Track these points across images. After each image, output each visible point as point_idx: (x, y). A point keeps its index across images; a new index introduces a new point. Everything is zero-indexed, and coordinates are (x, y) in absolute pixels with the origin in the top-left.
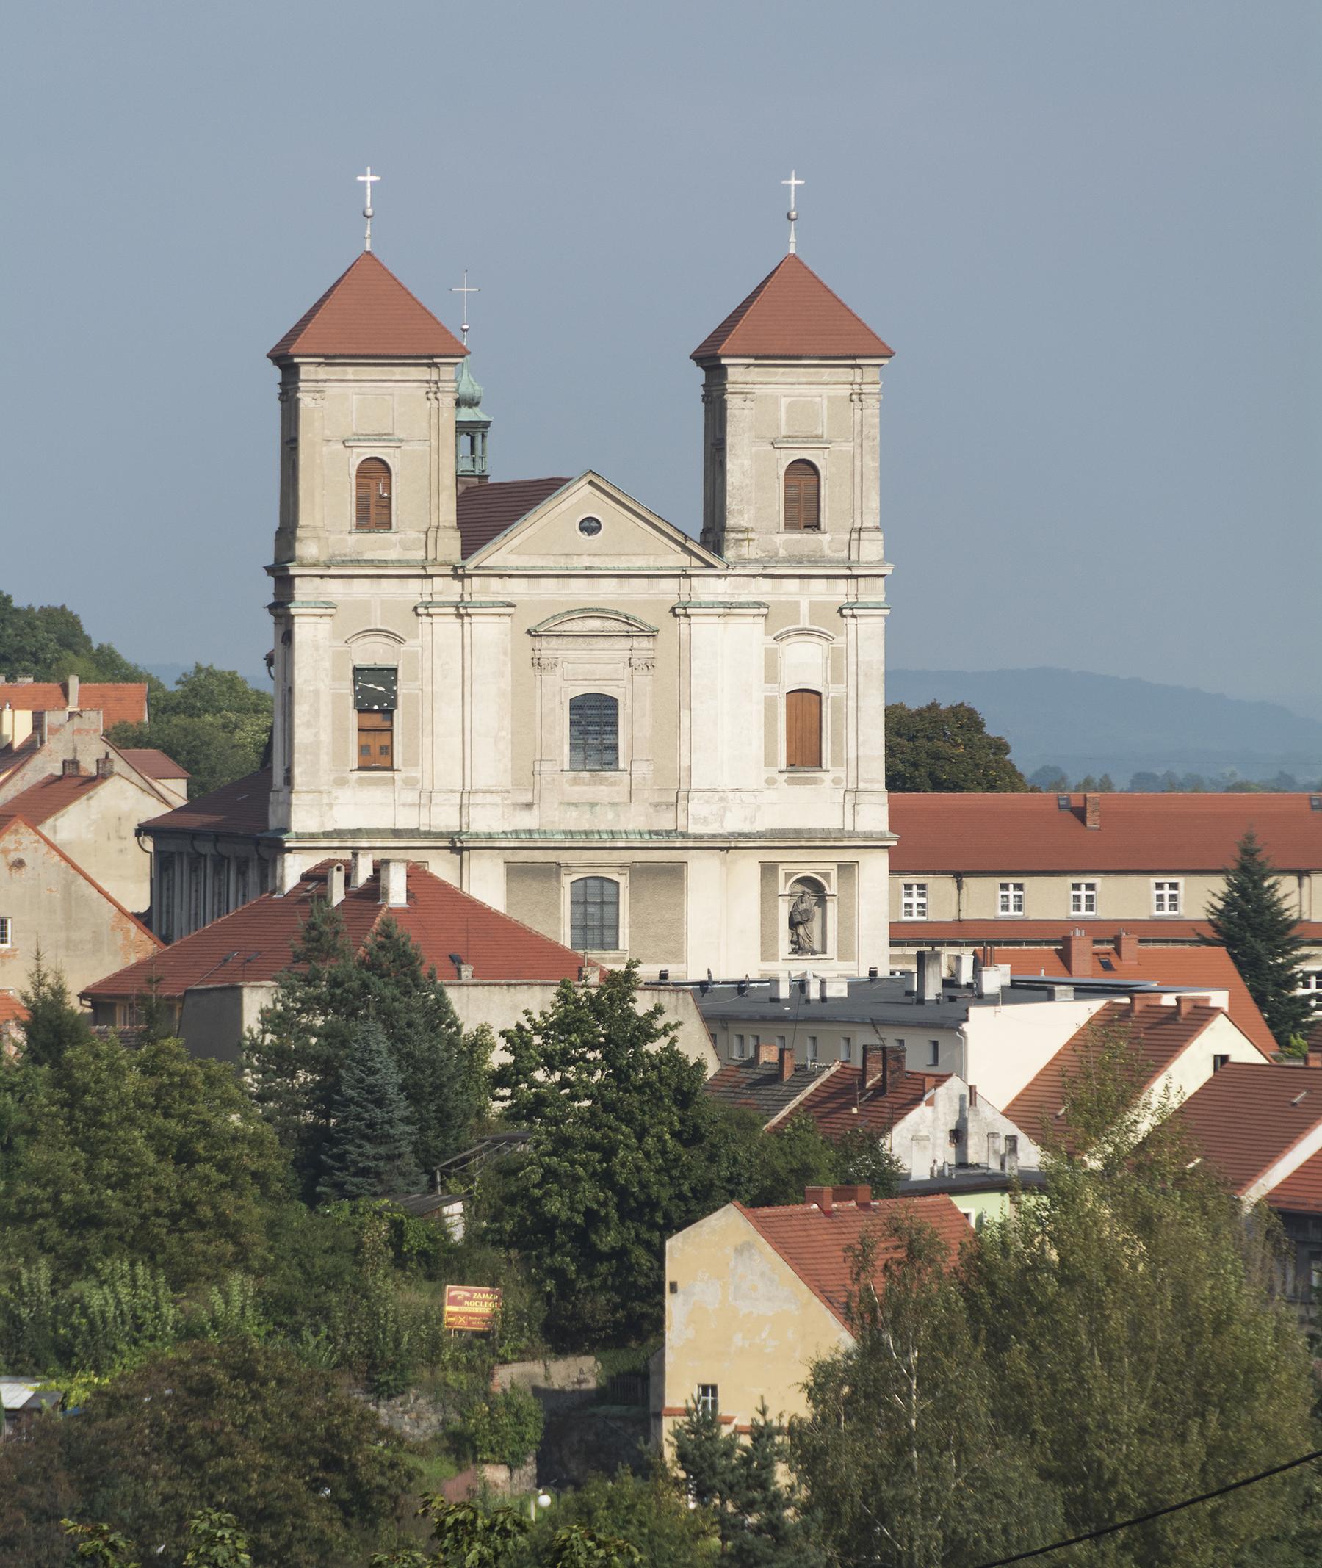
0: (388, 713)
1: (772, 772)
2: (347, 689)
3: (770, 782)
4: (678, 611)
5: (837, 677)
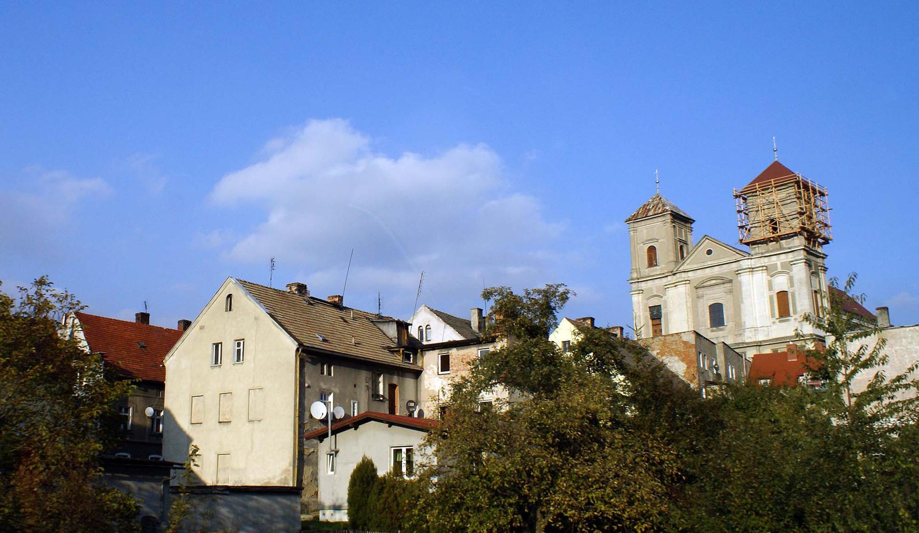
1: (774, 319)
2: (648, 314)
3: (774, 323)
5: (792, 285)
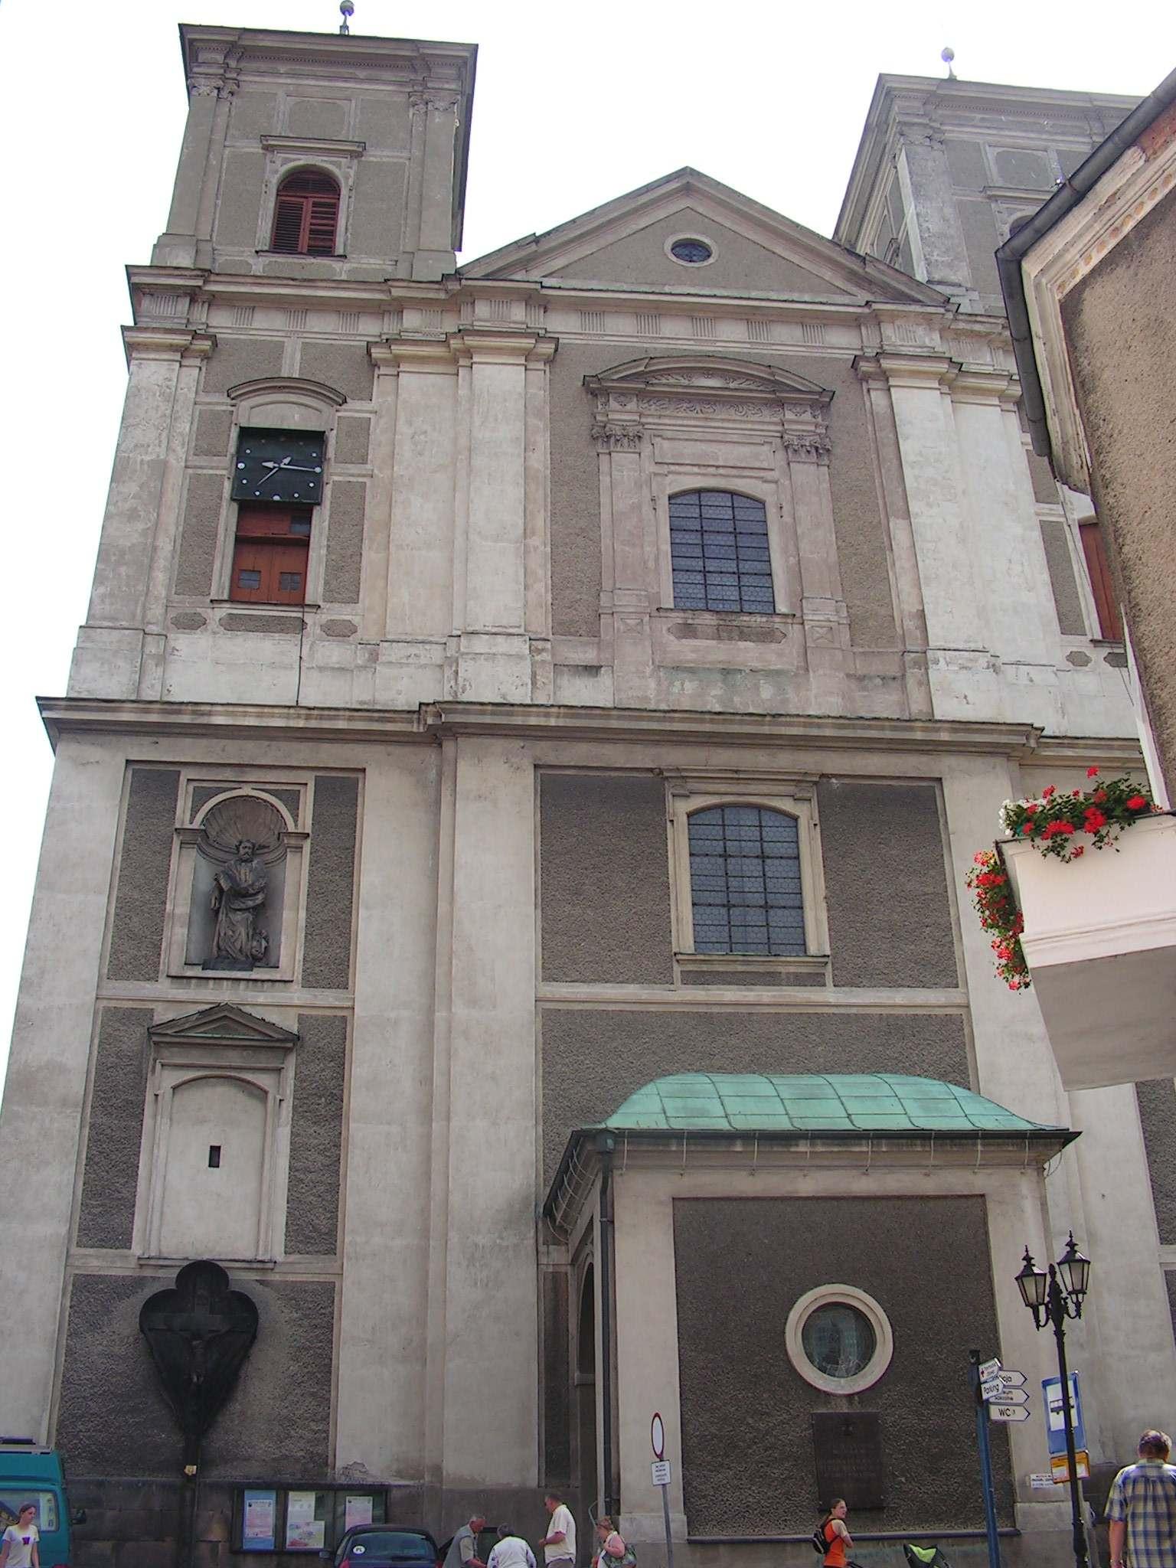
0: (303, 512)
1: (1079, 644)
2: (222, 468)
4: (865, 367)
